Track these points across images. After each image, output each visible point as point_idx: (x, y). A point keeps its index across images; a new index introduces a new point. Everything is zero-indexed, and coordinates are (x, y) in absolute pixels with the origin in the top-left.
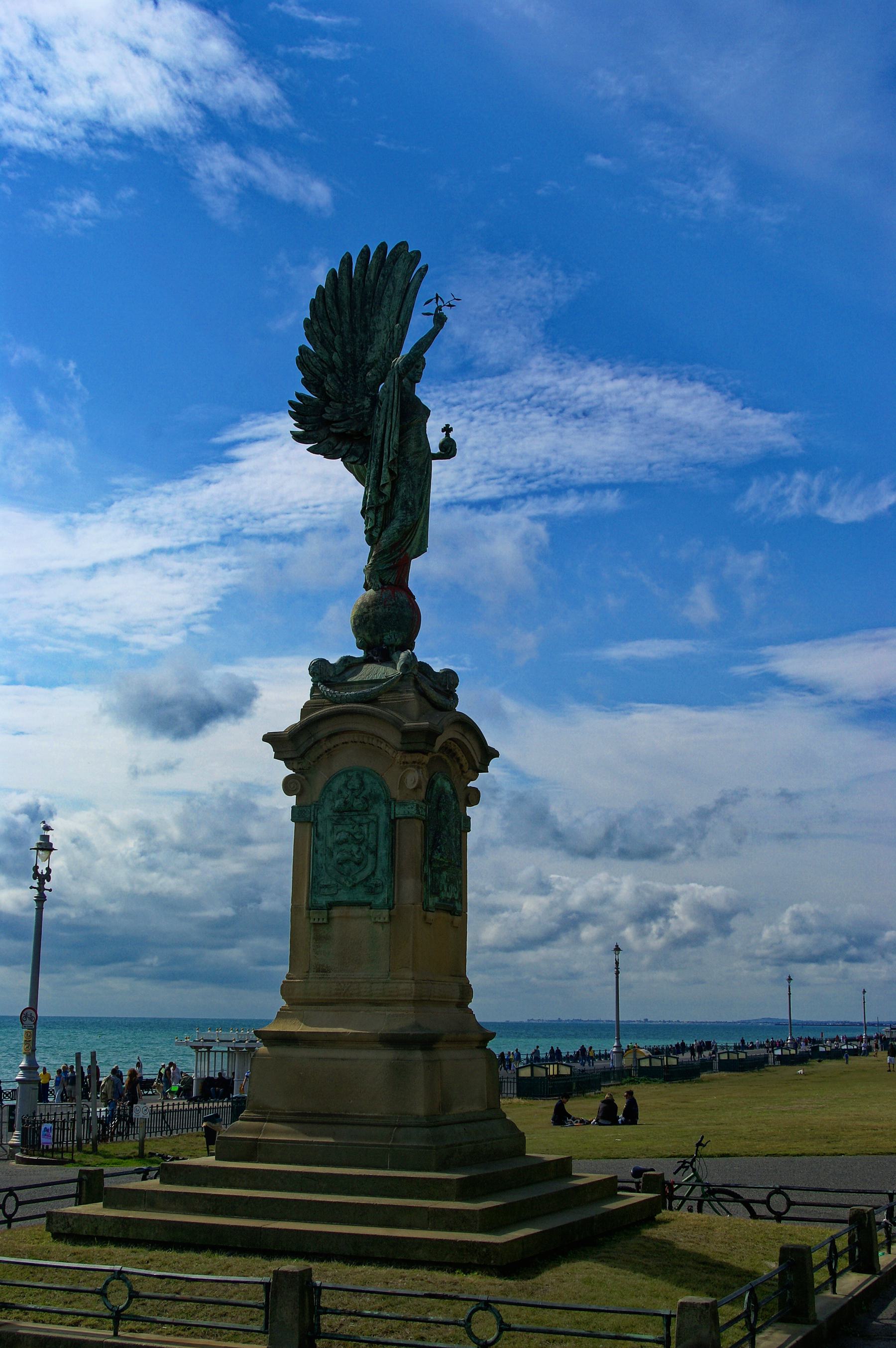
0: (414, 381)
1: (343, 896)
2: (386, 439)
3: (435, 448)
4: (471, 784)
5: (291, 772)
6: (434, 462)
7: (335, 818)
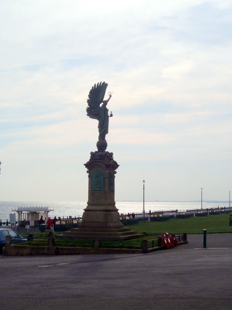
1: (96, 189)
5: (88, 170)
6: (109, 117)
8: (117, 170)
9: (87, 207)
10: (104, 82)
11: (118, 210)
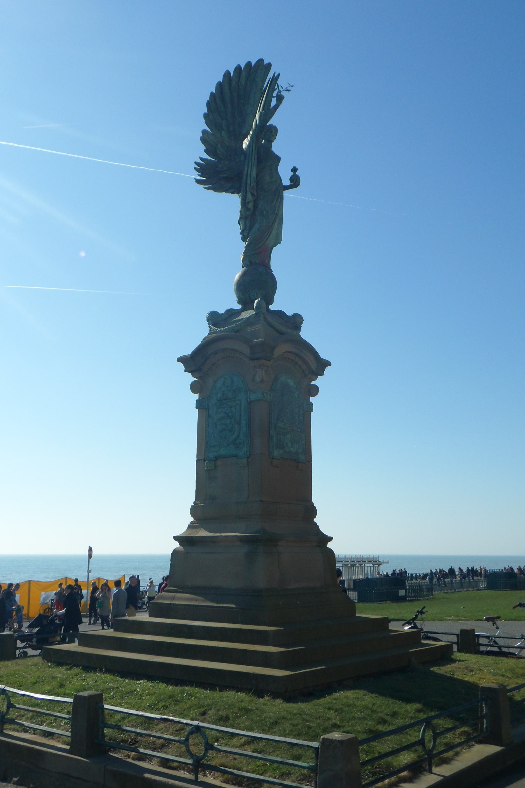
0: (270, 141)
1: (223, 452)
2: (249, 174)
3: (286, 182)
4: (313, 383)
5: (196, 379)
7: (218, 404)
8: (319, 382)
9: (191, 526)
10: (261, 61)
11: (331, 539)
